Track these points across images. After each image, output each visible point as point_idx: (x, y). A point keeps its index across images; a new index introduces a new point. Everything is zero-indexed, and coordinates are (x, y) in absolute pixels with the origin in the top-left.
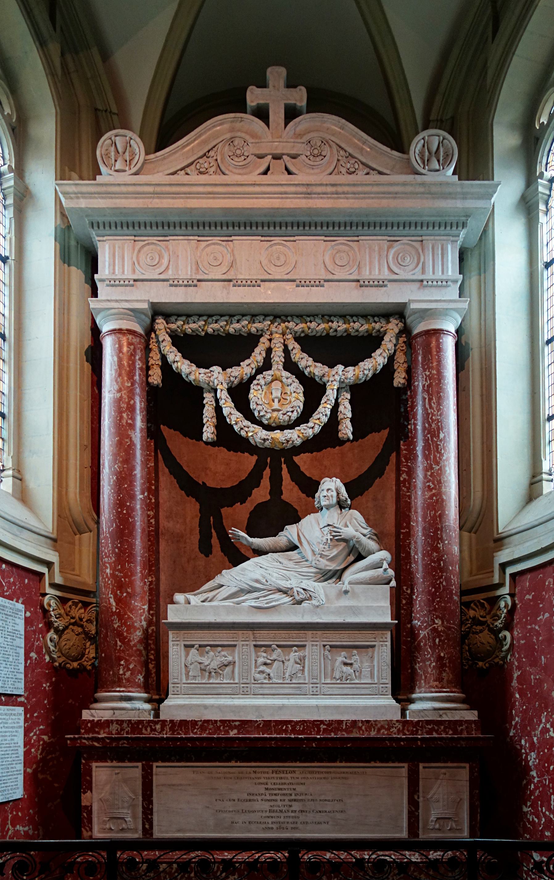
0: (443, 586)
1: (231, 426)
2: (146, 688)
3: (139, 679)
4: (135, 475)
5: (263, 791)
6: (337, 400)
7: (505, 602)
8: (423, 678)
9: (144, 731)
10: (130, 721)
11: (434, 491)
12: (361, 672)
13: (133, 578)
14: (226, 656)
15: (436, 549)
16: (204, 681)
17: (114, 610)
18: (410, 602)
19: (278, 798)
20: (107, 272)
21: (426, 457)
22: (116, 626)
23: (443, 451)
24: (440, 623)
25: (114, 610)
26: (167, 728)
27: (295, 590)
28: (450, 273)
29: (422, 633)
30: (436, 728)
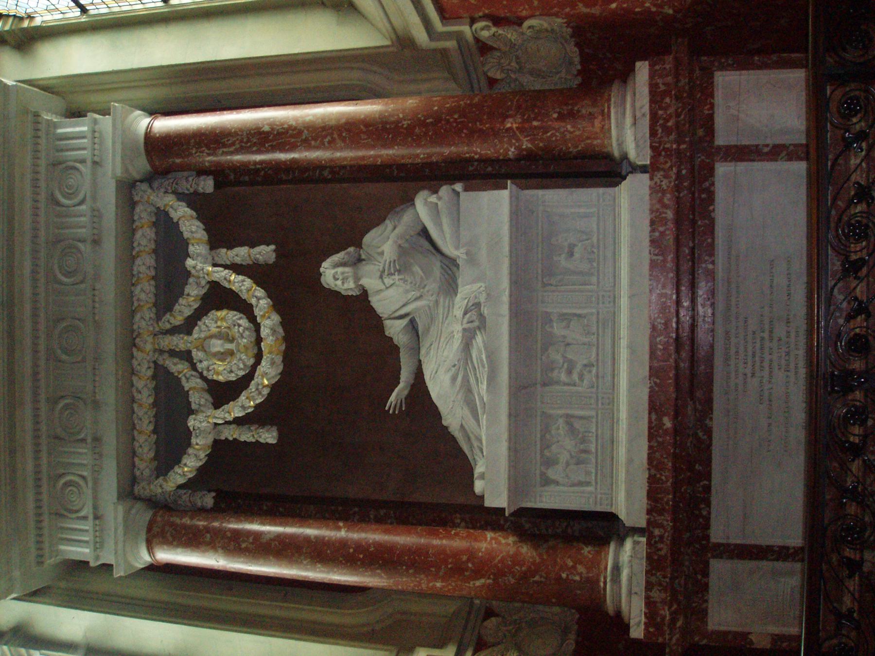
0: (460, 117)
1: (257, 406)
2: (602, 542)
3: (589, 552)
4: (316, 537)
5: (755, 382)
6: (226, 267)
7: (482, 29)
8: (589, 141)
9: (662, 553)
10: (647, 572)
11: (335, 136)
12: (583, 232)
13: (448, 552)
14: (560, 428)
15: (410, 130)
16: (594, 460)
17: (490, 581)
18: (485, 161)
19: (767, 357)
20: (87, 550)
21: (293, 148)
22: (513, 581)
23: (286, 126)
24: (511, 120)
25: (490, 581)
26: (660, 519)
27: (465, 326)
28: (85, 129)
29: (526, 144)
30: (661, 122)
